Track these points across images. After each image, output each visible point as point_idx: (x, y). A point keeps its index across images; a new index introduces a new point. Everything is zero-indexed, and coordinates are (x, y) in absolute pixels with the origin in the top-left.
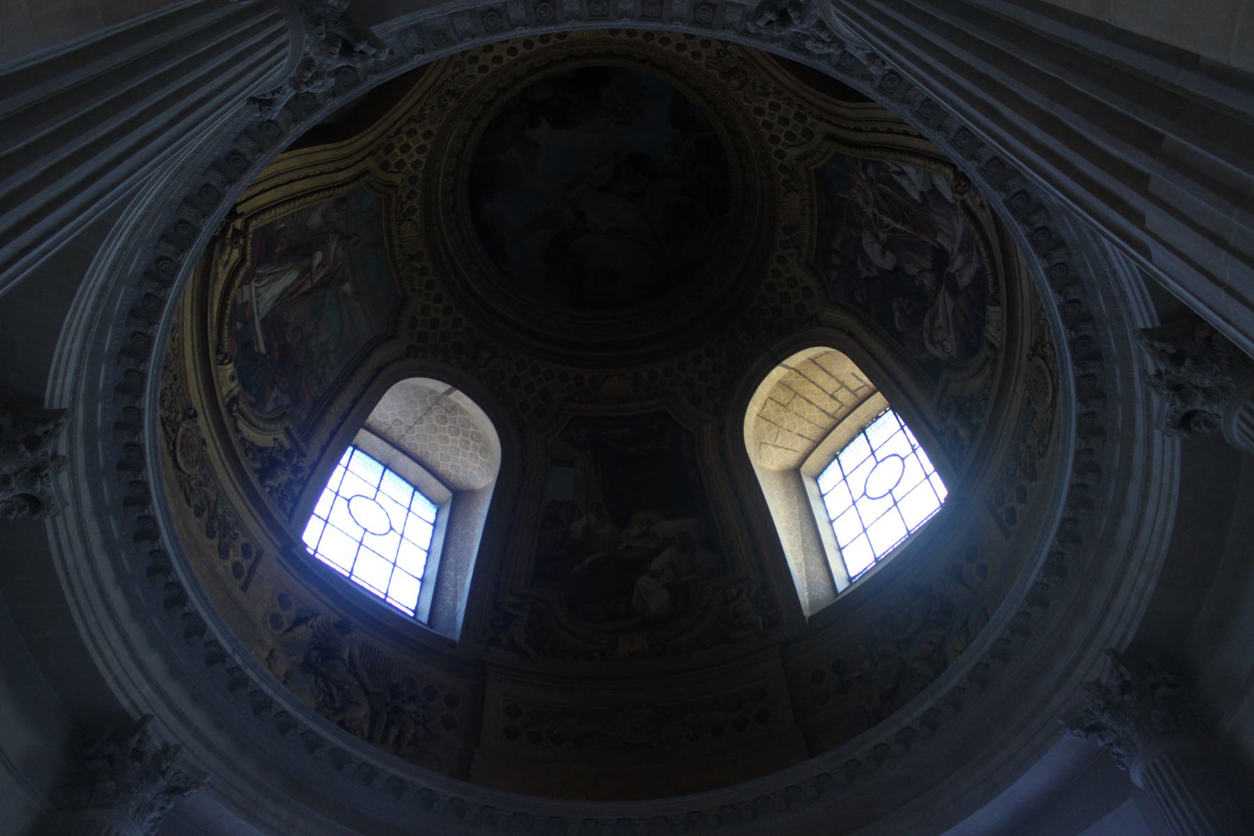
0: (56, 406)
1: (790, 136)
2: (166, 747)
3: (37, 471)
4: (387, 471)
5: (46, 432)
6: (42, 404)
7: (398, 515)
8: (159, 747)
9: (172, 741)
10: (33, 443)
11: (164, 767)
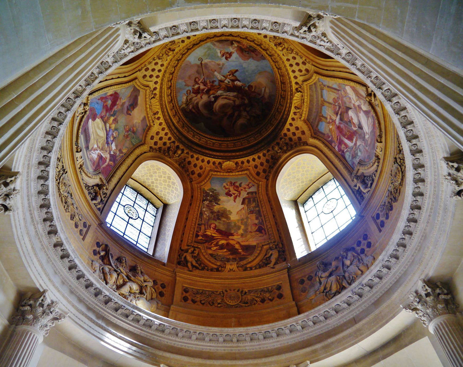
0: (16, 171)
1: (300, 71)
2: (53, 302)
3: (7, 196)
4: (138, 195)
5: (11, 181)
6: (11, 170)
7: (141, 213)
8: (50, 302)
9: (55, 299)
10: (6, 184)
11: (52, 310)
